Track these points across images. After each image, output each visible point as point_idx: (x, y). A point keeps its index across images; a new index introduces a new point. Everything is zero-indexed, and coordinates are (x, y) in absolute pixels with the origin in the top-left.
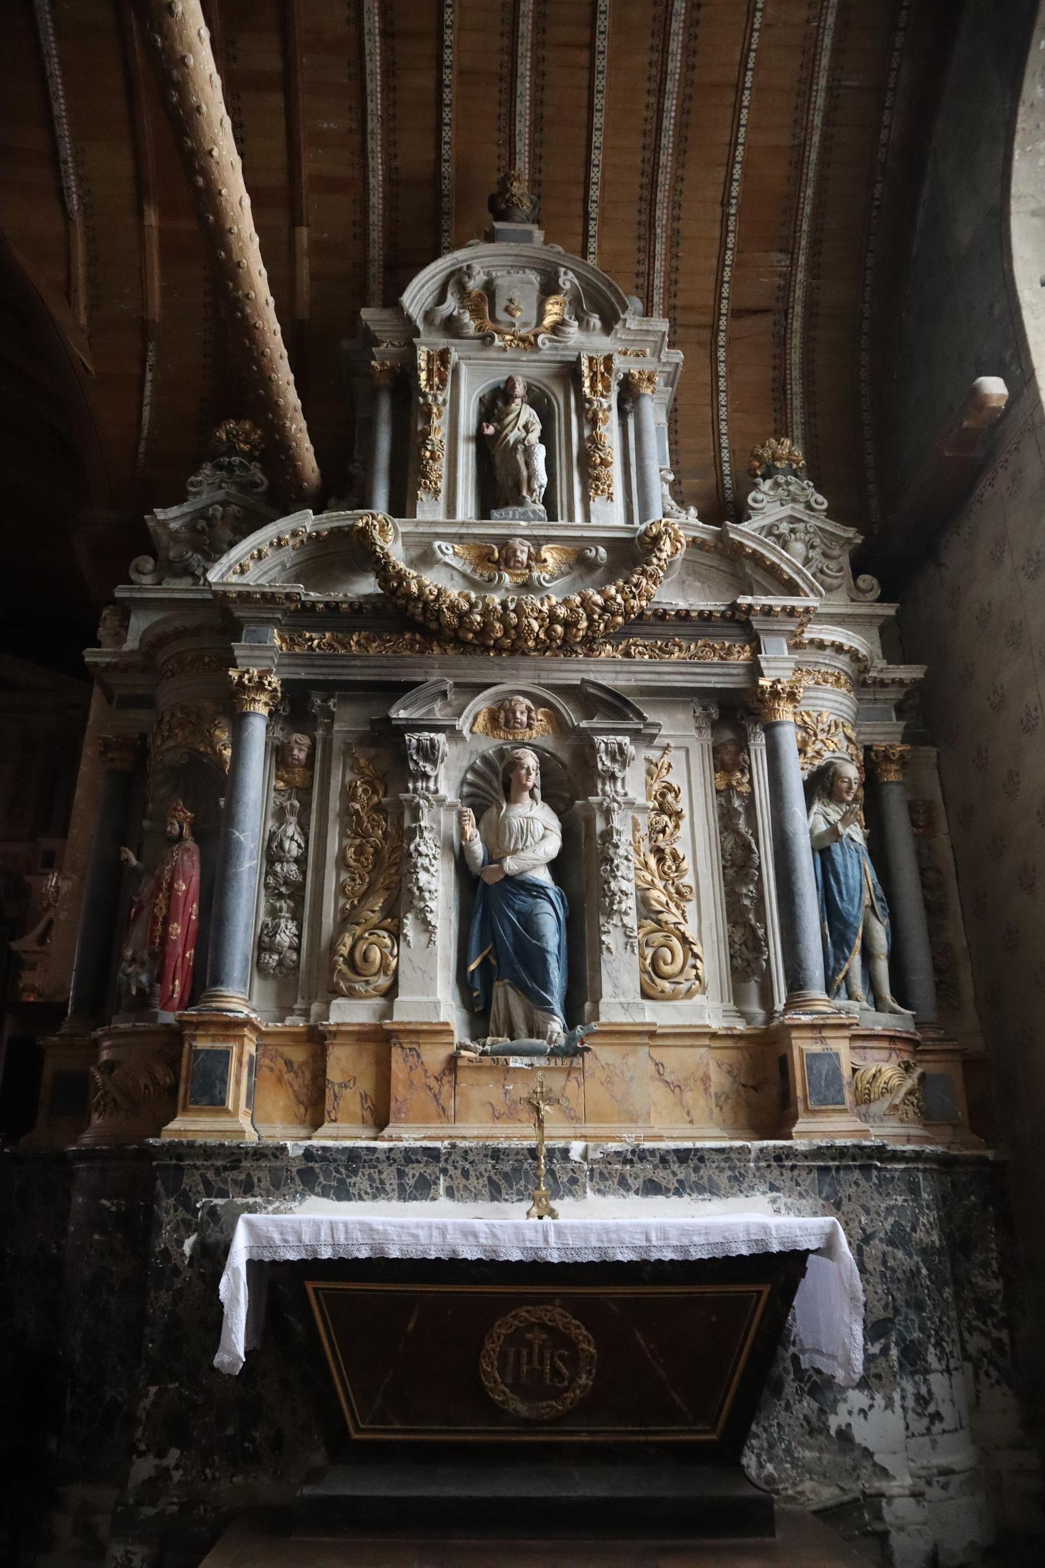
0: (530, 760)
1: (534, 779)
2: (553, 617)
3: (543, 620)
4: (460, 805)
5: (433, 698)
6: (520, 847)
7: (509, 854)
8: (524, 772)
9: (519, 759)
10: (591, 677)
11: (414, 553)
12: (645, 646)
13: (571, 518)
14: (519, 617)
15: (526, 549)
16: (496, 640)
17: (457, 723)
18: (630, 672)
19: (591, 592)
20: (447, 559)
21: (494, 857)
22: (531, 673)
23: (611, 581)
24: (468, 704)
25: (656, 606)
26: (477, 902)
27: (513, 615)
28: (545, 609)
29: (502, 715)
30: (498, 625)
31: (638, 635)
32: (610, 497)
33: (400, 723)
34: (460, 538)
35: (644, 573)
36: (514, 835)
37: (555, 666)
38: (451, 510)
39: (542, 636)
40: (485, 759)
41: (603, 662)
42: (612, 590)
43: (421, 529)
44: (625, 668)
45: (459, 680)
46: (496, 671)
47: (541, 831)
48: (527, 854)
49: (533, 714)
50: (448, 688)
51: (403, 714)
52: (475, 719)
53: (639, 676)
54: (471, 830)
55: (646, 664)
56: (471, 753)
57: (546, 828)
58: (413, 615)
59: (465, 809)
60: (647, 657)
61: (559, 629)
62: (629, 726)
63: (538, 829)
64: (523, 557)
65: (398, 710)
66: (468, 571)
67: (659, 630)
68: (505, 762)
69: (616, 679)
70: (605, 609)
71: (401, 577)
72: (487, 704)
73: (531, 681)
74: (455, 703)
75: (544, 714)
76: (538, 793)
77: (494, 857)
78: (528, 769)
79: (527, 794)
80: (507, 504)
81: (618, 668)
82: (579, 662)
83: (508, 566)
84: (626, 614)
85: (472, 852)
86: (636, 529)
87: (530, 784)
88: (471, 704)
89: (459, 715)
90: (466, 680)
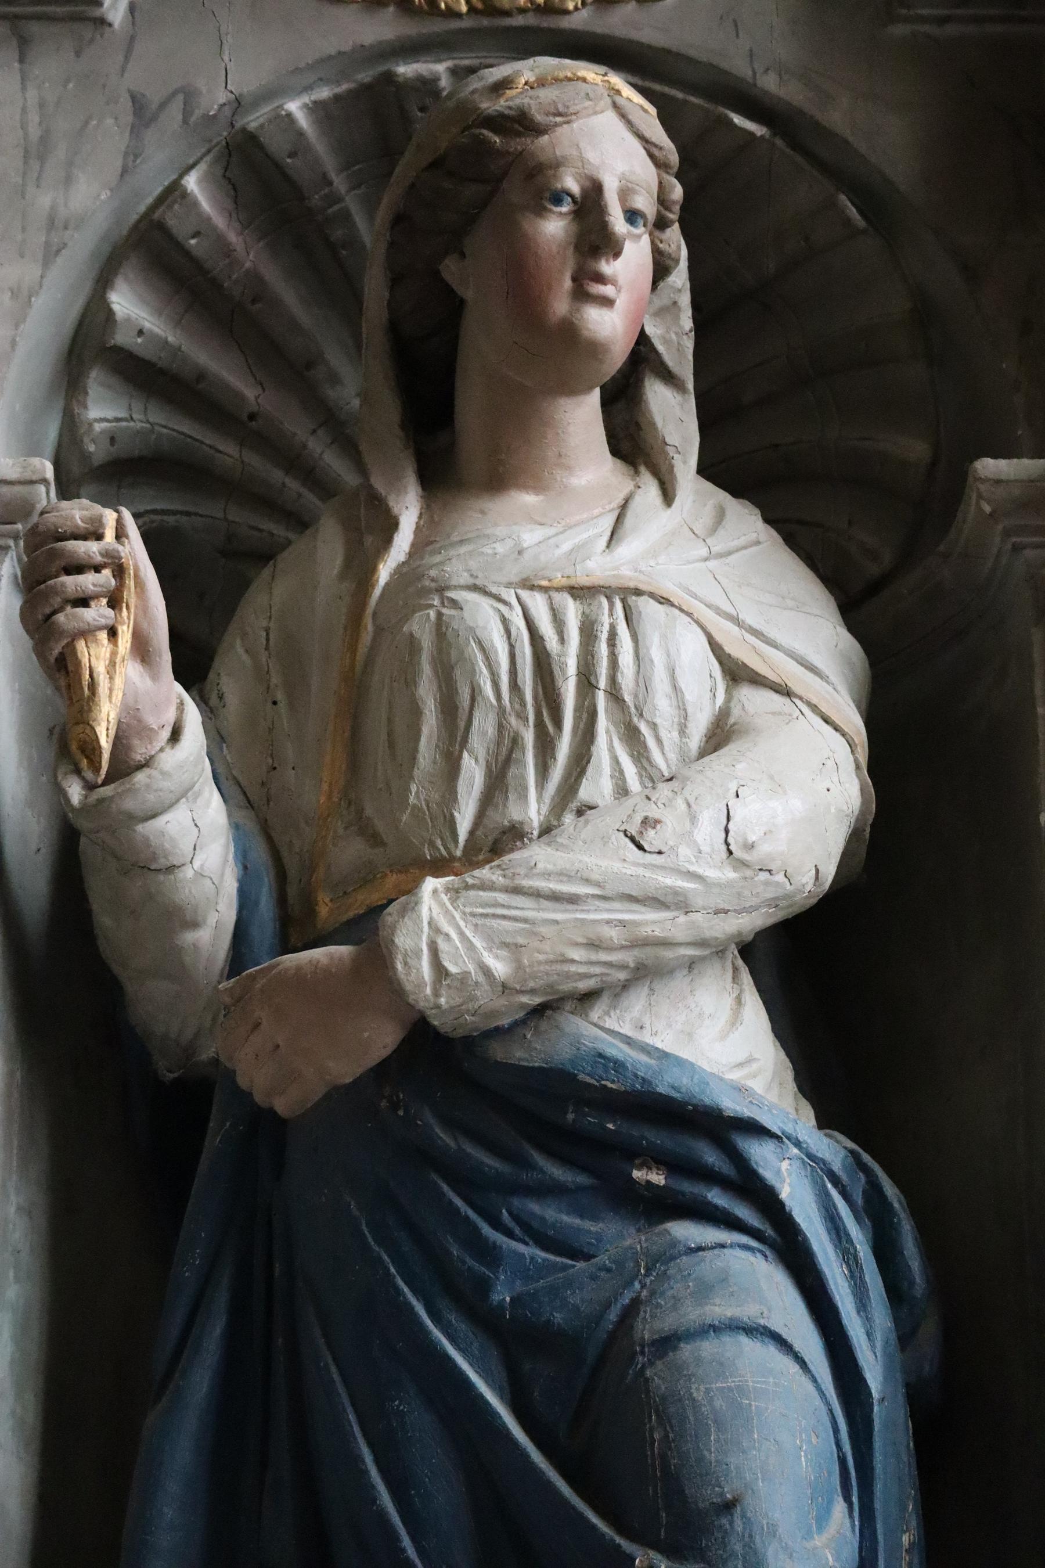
0: (610, 140)
1: (634, 297)
4: (45, 496)
6: (533, 811)
7: (439, 867)
8: (554, 227)
9: (522, 124)
21: (319, 886)
26: (190, 1262)
36: (483, 729)
40: (249, 162)
47: (702, 690)
48: (587, 856)
54: (128, 681)
56: (142, 114)
57: (736, 673)
59: (78, 511)
63: (676, 677)
68: (408, 166)
76: (672, 413)
77: (319, 886)
78: (589, 206)
79: (582, 418)
85: (148, 867)
87: (609, 325)
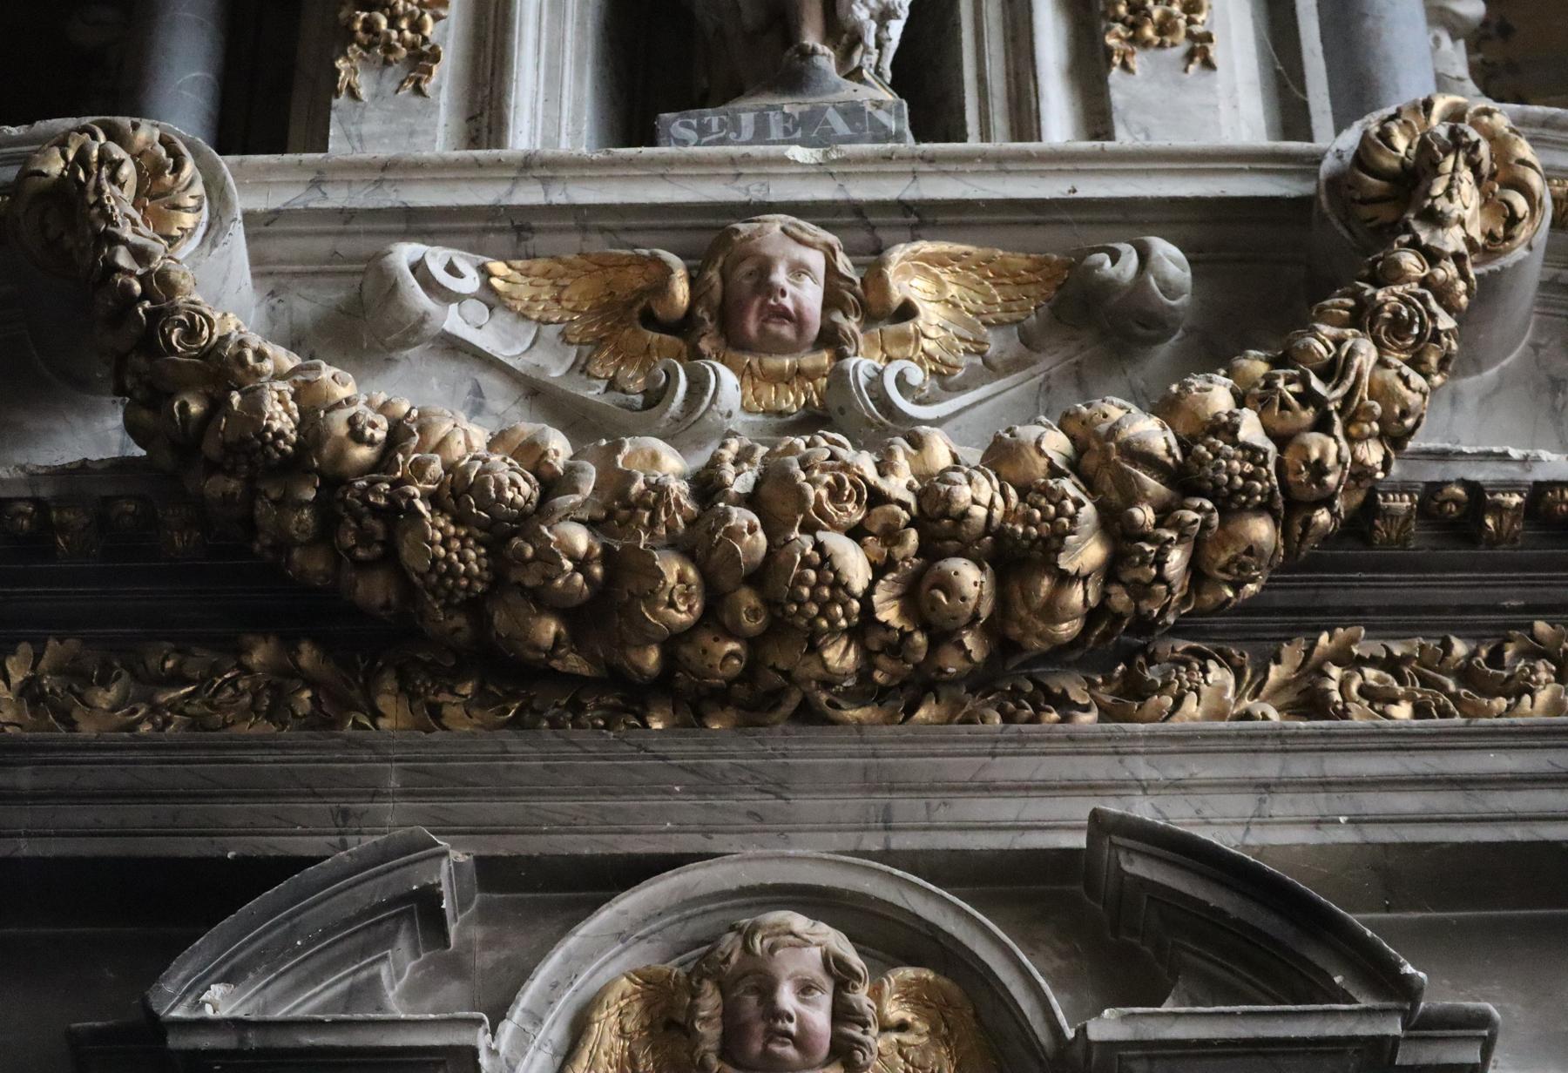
2: (936, 517)
3: (891, 535)
5: (368, 932)
10: (1142, 809)
11: (305, 306)
12: (1391, 665)
13: (1025, 121)
14: (774, 527)
15: (816, 260)
16: (674, 641)
17: (482, 1040)
18: (1325, 785)
19: (1114, 409)
20: (453, 321)
22: (852, 805)
23: (1214, 354)
24: (541, 954)
25: (1435, 472)
27: (741, 517)
28: (899, 485)
29: (710, 1002)
30: (671, 568)
31: (1354, 614)
32: (1199, 51)
33: (206, 1042)
34: (510, 229)
35: (1363, 316)
37: (960, 768)
38: (484, 115)
39: (888, 613)
41: (1190, 743)
42: (1219, 396)
43: (338, 198)
44: (1302, 767)
45: (503, 847)
46: (687, 806)
49: (861, 996)
50: (443, 877)
51: (220, 1002)
52: (579, 1027)
53: (1372, 803)
55: (1400, 741)
58: (283, 545)
60: (1402, 711)
61: (970, 577)
62: (1333, 1029)
64: (809, 296)
65: (201, 984)
66: (555, 370)
67: (1450, 590)
69: (1262, 820)
70: (1184, 479)
71: (223, 369)
72: (639, 956)
73: (850, 840)
74: (485, 959)
75: (912, 995)
80: (727, 91)
81: (1269, 767)
82: (1079, 744)
83: (734, 342)
84: (1290, 507)
86: (1316, 159)
88: (557, 957)
89: (498, 1014)
90: (534, 845)
